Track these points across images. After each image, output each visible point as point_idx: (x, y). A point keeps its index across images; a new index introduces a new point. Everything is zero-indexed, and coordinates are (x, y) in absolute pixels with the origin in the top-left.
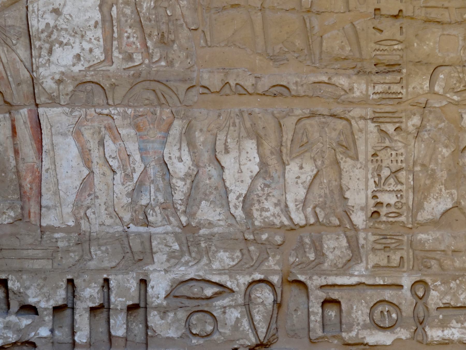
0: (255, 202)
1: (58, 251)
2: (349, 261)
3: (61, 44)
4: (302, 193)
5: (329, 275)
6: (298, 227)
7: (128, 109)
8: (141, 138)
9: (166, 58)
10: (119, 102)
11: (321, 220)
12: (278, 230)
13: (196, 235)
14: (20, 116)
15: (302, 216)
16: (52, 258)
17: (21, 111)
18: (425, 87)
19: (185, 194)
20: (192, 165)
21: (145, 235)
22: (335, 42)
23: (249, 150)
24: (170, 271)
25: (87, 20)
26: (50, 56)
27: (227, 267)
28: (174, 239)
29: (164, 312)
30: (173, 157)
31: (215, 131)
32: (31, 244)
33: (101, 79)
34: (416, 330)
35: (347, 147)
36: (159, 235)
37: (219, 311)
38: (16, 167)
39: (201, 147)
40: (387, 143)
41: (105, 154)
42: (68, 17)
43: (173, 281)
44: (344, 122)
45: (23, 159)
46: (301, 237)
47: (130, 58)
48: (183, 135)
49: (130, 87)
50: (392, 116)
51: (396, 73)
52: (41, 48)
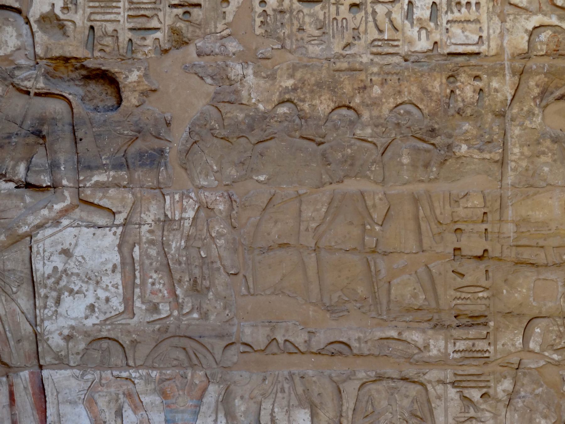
3: (71, 291)
7: (152, 371)
8: (168, 407)
9: (199, 309)
10: (141, 363)
14: (19, 380)
18: (517, 344)
22: (406, 289)
25: (102, 263)
26: (57, 307)
31: (260, 398)
33: (119, 335)
39: (242, 419)
40: (472, 413)
42: (80, 259)
44: (419, 387)
47: (155, 308)
48: (219, 403)
49: (155, 344)
50: (477, 380)
51: (481, 327)
52: (46, 297)
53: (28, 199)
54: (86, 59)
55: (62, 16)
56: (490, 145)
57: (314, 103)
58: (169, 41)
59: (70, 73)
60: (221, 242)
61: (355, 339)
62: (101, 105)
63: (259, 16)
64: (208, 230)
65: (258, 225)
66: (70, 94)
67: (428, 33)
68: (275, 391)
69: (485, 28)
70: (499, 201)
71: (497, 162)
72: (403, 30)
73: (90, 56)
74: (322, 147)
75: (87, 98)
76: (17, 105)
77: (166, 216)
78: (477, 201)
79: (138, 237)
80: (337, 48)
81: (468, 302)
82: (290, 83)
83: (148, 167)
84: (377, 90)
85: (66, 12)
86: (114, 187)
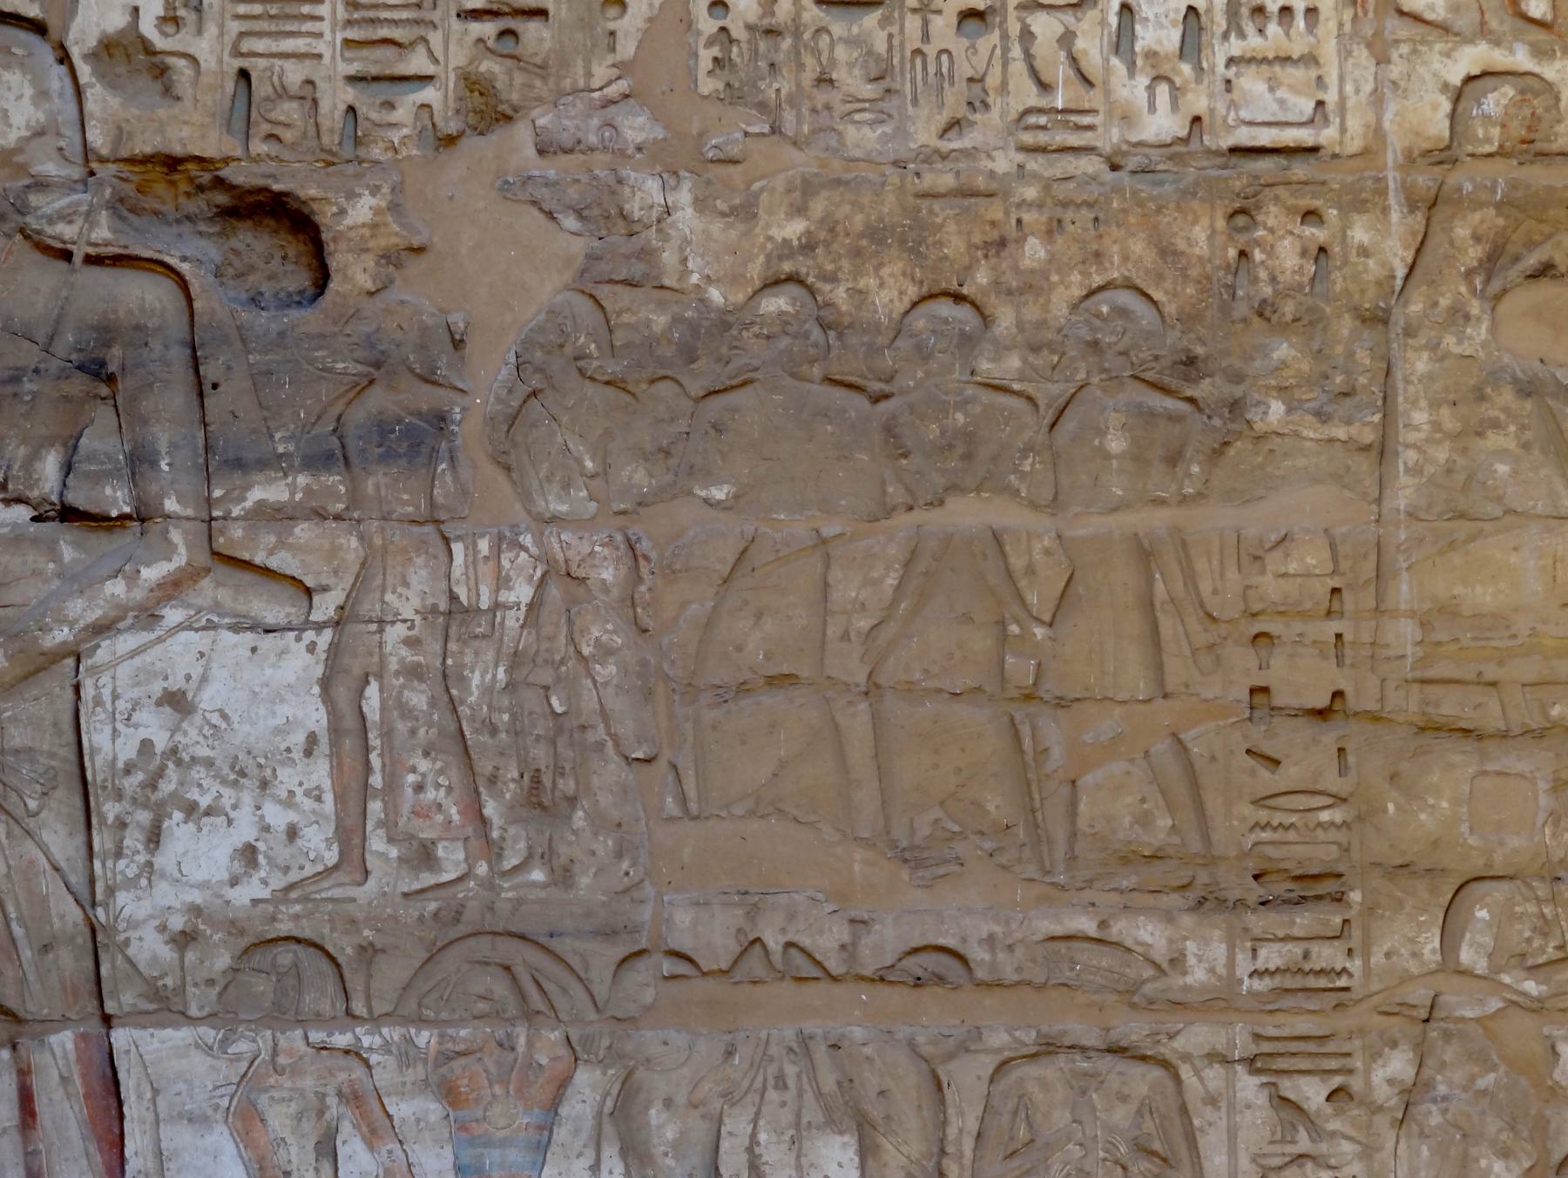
8: (462, 1131)
9: (548, 857)
10: (388, 1008)
14: (48, 1057)
17: (54, 1039)
18: (1427, 951)
22: (1118, 802)
25: (278, 731)
26: (152, 852)
33: (326, 931)
39: (670, 1162)
40: (1304, 1143)
42: (215, 719)
44: (1157, 1073)
47: (425, 856)
48: (606, 1119)
49: (425, 955)
50: (1316, 1051)
52: (122, 825)
53: (68, 553)
54: (227, 160)
55: (160, 43)
56: (1348, 402)
57: (862, 284)
58: (458, 111)
59: (182, 200)
60: (607, 671)
61: (981, 941)
62: (267, 288)
63: (709, 44)
64: (571, 639)
65: (709, 624)
66: (184, 259)
67: (1176, 92)
68: (758, 1084)
69: (1332, 79)
70: (1373, 557)
71: (1366, 448)
72: (1106, 82)
73: (238, 153)
74: (883, 406)
75: (231, 271)
76: (37, 288)
77: (453, 598)
78: (1313, 558)
79: (376, 659)
80: (924, 133)
81: (1291, 836)
82: (794, 229)
83: (403, 462)
84: (1034, 251)
85: (170, 29)
86: (307, 518)
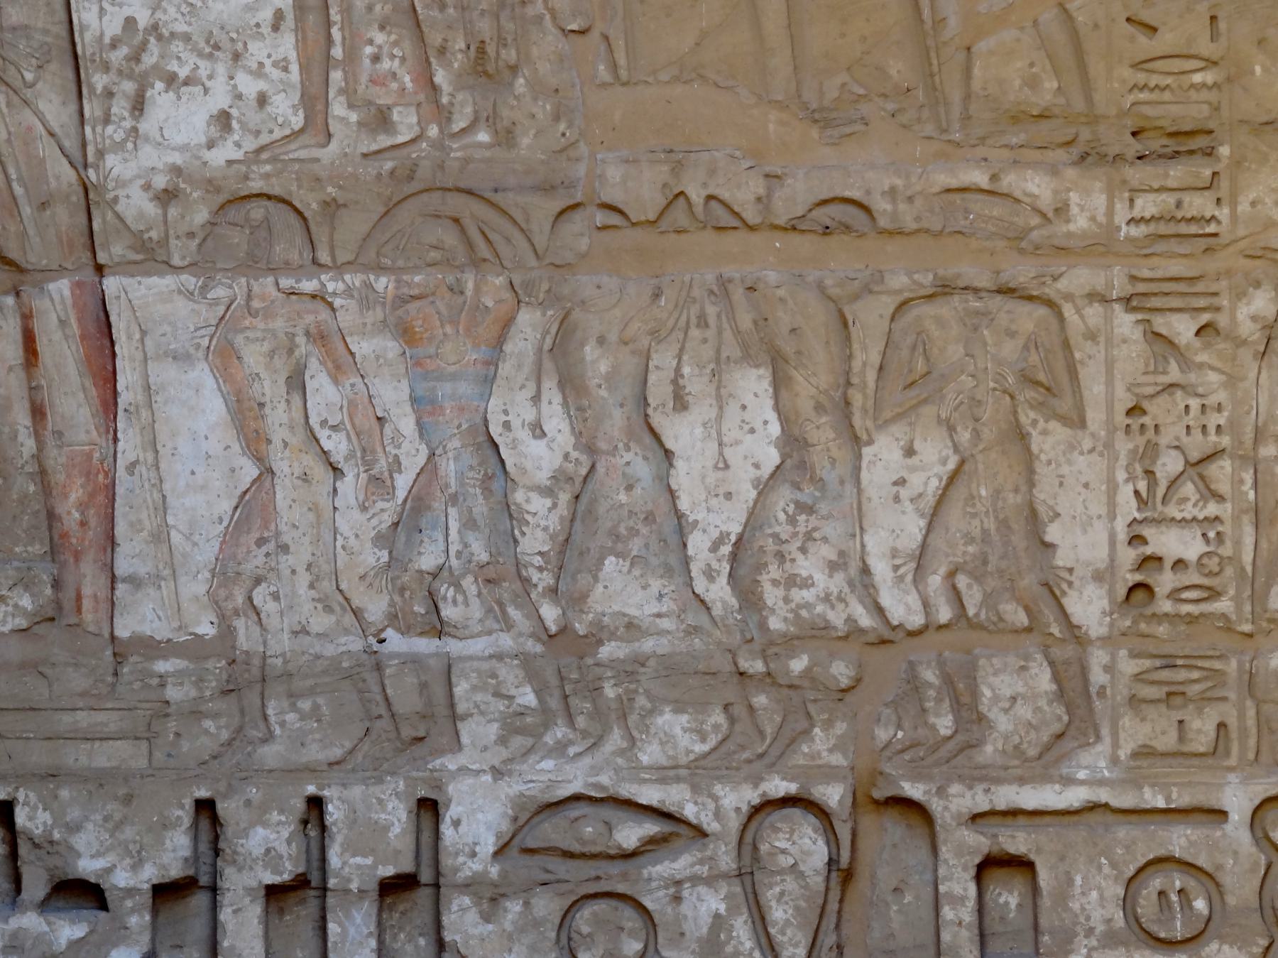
0: (769, 558)
1: (167, 715)
2: (1060, 736)
3: (171, 80)
4: (912, 528)
5: (999, 781)
6: (900, 635)
7: (378, 277)
8: (418, 366)
9: (492, 120)
10: (351, 257)
11: (971, 612)
12: (840, 644)
13: (590, 661)
15: (913, 600)
16: (149, 736)
19: (551, 538)
20: (575, 447)
21: (432, 662)
22: (1010, 66)
23: (748, 399)
24: (510, 773)
26: (137, 119)
27: (684, 760)
28: (521, 673)
29: (491, 898)
30: (516, 423)
31: (645, 341)
32: (83, 695)
33: (294, 188)
34: (1268, 948)
35: (1051, 384)
36: (475, 664)
37: (661, 893)
38: (38, 457)
39: (603, 393)
40: (1174, 373)
41: (307, 417)
43: (519, 802)
44: (1042, 311)
45: (59, 434)
46: (912, 665)
47: (381, 120)
48: (546, 356)
49: (382, 210)
51: (1198, 159)
52: (109, 94)
61: (883, 193)
81: (1167, 96)
